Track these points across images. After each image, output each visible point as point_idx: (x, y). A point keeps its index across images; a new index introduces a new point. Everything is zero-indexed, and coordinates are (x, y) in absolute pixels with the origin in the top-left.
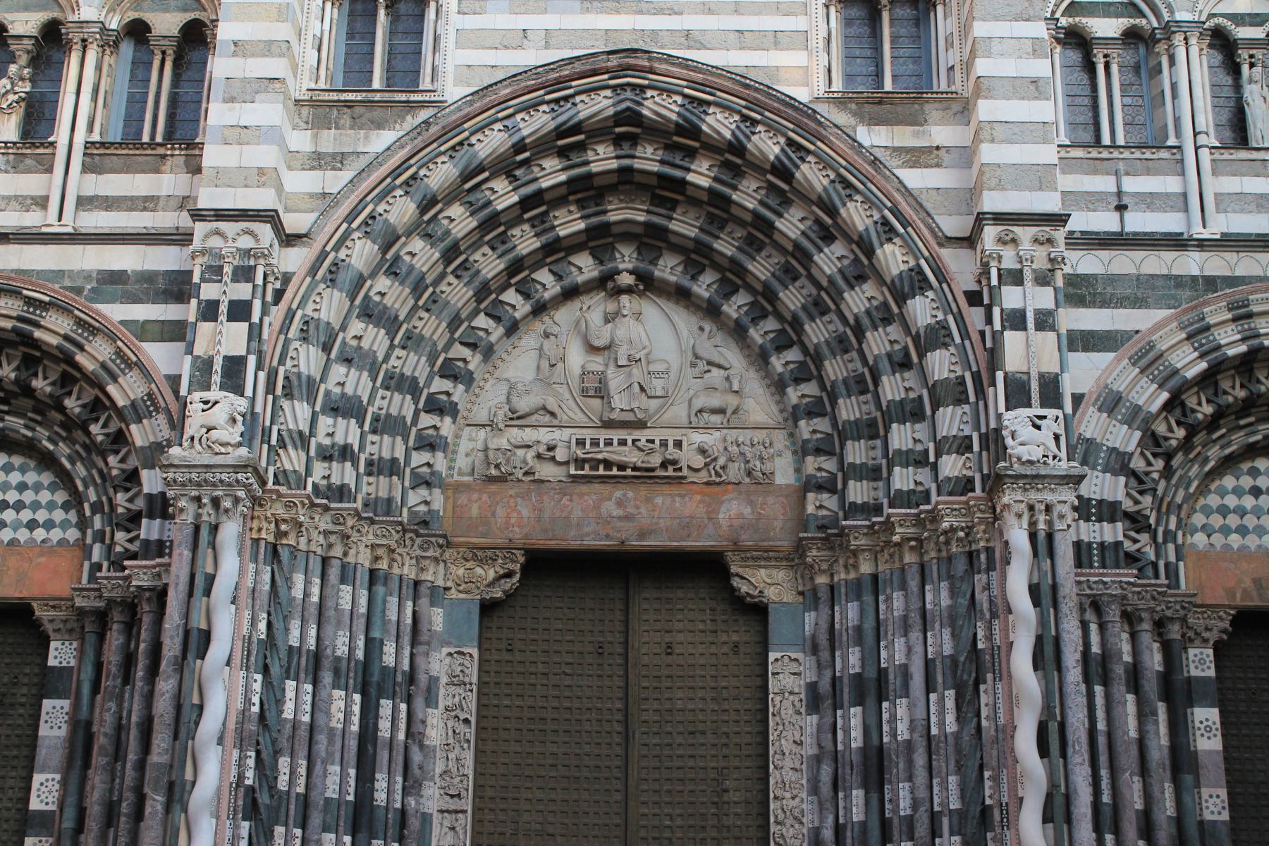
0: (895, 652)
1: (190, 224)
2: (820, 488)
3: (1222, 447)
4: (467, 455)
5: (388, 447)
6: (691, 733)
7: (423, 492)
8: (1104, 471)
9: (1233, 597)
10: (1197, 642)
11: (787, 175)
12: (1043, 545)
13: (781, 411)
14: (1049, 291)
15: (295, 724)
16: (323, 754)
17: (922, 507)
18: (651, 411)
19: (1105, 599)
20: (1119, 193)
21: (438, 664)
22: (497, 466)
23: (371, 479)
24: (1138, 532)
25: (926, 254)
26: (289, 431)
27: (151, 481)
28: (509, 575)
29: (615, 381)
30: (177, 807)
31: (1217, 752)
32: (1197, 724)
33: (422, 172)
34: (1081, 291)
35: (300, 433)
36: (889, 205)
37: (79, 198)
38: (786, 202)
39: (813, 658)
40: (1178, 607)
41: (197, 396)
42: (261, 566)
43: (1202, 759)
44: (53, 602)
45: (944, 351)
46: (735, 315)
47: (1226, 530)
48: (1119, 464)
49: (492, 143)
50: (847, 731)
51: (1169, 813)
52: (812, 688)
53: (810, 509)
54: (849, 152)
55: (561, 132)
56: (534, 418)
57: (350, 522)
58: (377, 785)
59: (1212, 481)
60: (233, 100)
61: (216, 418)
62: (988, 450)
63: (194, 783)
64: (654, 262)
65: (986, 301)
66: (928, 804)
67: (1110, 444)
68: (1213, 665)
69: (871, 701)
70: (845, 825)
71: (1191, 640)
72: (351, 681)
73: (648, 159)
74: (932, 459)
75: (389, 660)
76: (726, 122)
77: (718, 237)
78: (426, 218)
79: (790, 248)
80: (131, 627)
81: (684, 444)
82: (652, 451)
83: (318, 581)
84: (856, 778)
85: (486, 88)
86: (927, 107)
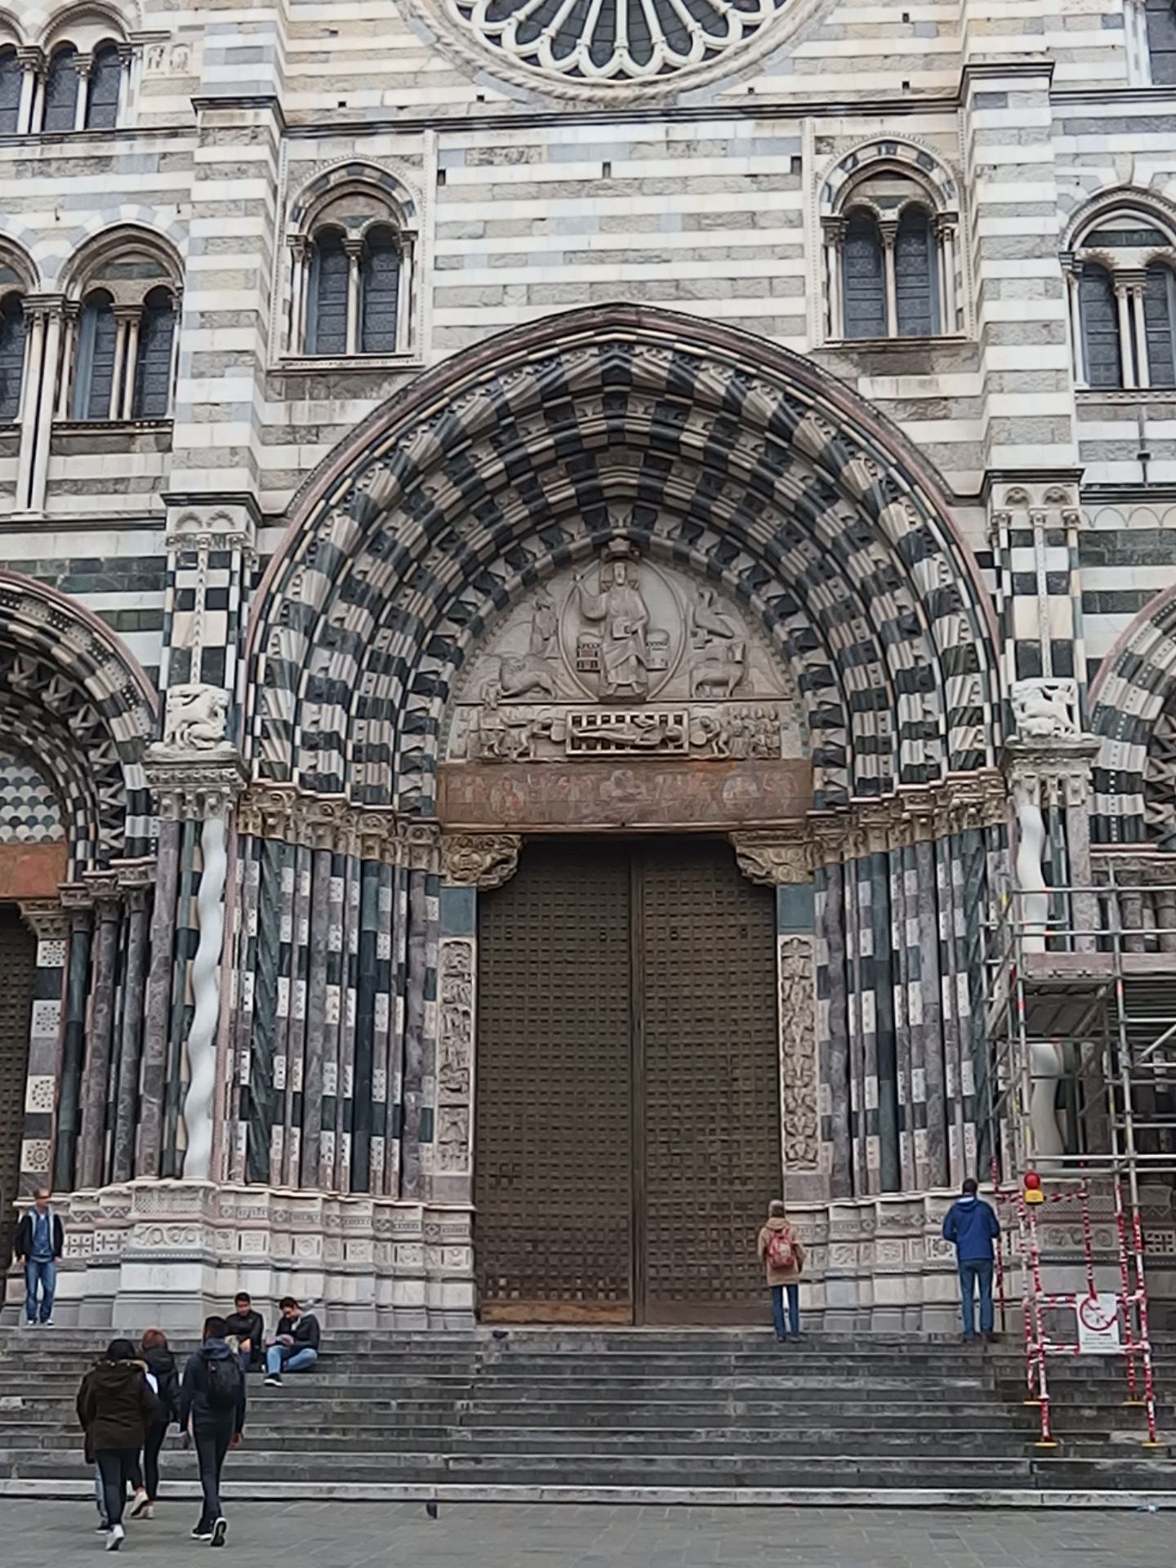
0: (909, 933)
1: (163, 506)
2: (829, 763)
4: (460, 736)
5: (377, 732)
6: (699, 1020)
7: (414, 777)
8: (1123, 740)
11: (788, 436)
12: (1055, 819)
13: (788, 681)
14: (1063, 550)
15: (289, 1020)
16: (319, 1051)
17: (933, 783)
18: (650, 684)
20: (1143, 442)
21: (435, 955)
22: (491, 748)
23: (360, 767)
24: (1161, 802)
25: (934, 513)
26: (274, 721)
27: (135, 777)
28: (506, 861)
29: (610, 655)
30: (172, 1110)
33: (402, 443)
35: (285, 723)
36: (894, 461)
37: (48, 483)
38: (787, 461)
39: (824, 941)
41: (177, 689)
42: (250, 862)
44: (41, 901)
45: (953, 617)
46: (736, 581)
48: (1141, 732)
49: (472, 409)
50: (859, 1018)
52: (822, 970)
53: (818, 785)
54: (850, 405)
55: (548, 393)
56: (529, 694)
57: (338, 814)
58: (375, 1081)
60: (201, 375)
61: (197, 709)
62: (1000, 720)
63: (189, 1086)
64: (650, 526)
65: (997, 563)
66: (941, 1091)
67: (1129, 711)
69: (882, 985)
70: (856, 1114)
72: (345, 977)
73: (639, 418)
74: (942, 731)
75: (384, 952)
76: (720, 378)
77: (715, 499)
78: (408, 490)
79: (792, 508)
80: (120, 925)
81: (685, 720)
82: (651, 729)
83: (307, 874)
84: (870, 1066)
85: (465, 351)
86: (934, 354)
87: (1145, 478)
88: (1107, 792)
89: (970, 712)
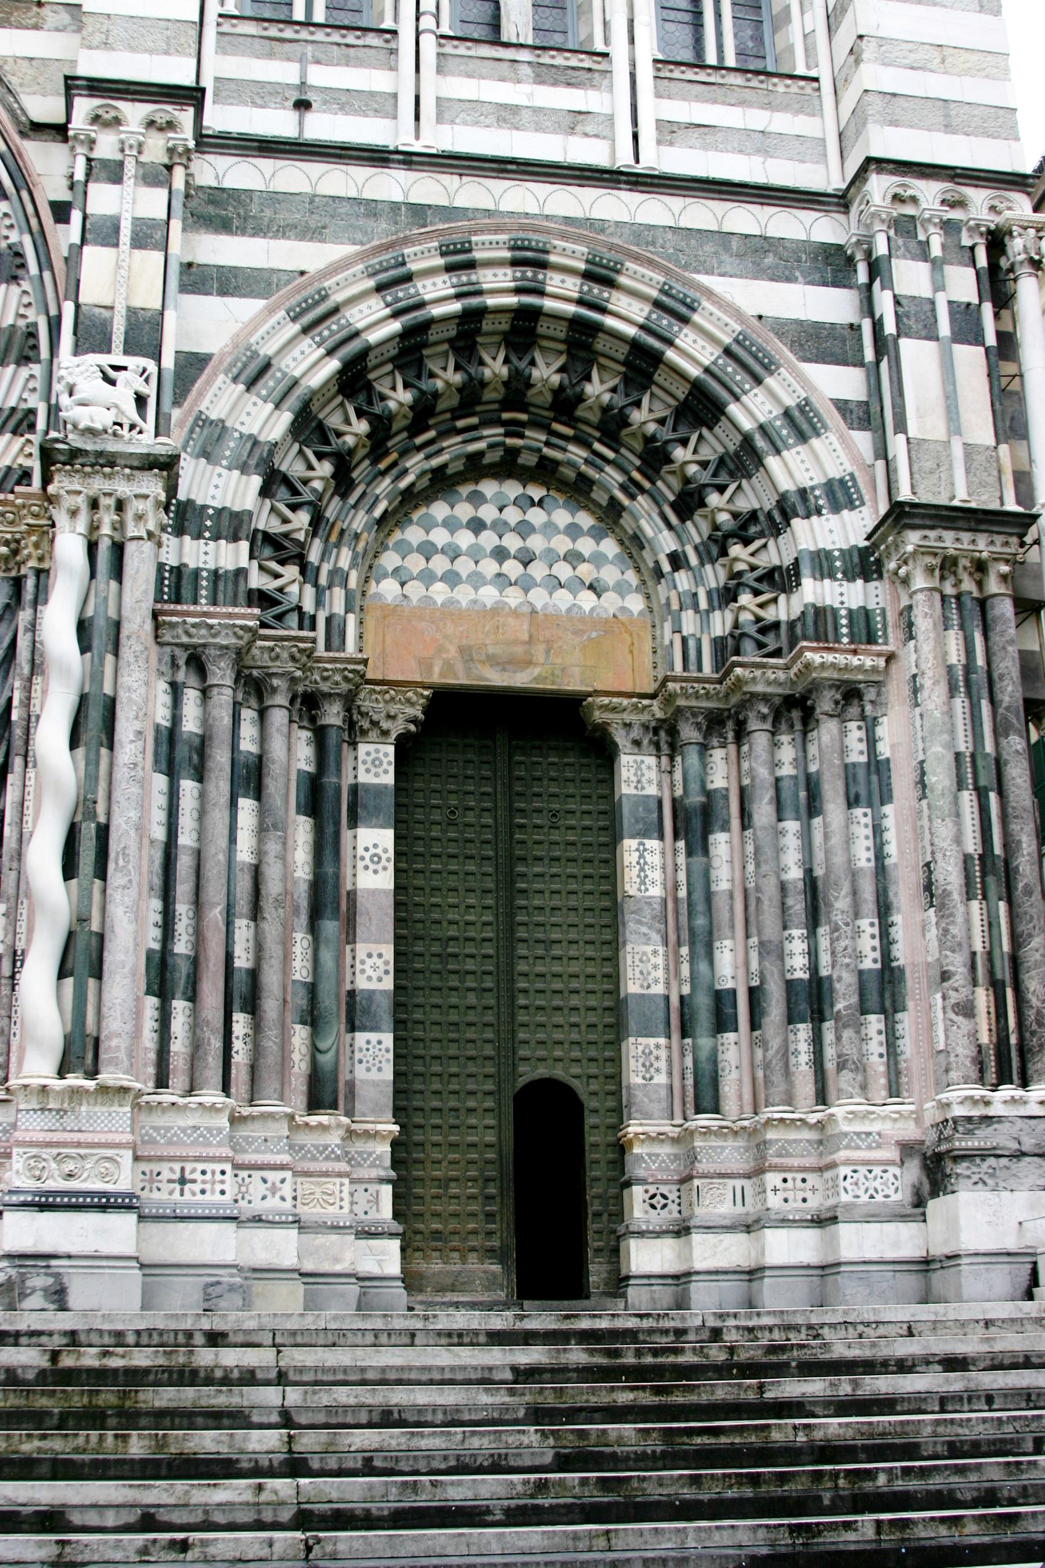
3: (428, 457)
8: (229, 468)
9: (430, 668)
10: (373, 735)
12: (109, 558)
19: (213, 652)
24: (282, 563)
31: (384, 891)
32: (360, 851)
34: (217, 211)
40: (338, 678)
43: (363, 903)
47: (428, 578)
51: (297, 977)
59: (416, 507)
67: (245, 430)
68: (392, 769)
71: (364, 732)
87: (301, 131)
88: (199, 536)
89: (18, 416)
